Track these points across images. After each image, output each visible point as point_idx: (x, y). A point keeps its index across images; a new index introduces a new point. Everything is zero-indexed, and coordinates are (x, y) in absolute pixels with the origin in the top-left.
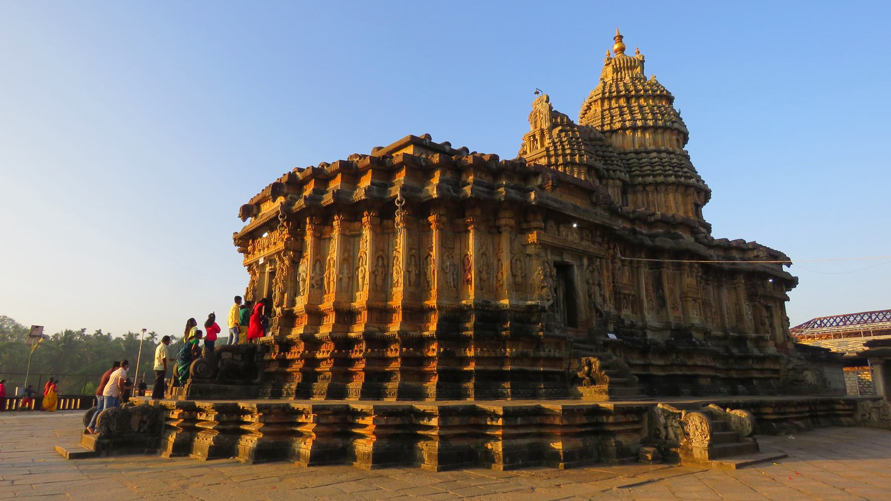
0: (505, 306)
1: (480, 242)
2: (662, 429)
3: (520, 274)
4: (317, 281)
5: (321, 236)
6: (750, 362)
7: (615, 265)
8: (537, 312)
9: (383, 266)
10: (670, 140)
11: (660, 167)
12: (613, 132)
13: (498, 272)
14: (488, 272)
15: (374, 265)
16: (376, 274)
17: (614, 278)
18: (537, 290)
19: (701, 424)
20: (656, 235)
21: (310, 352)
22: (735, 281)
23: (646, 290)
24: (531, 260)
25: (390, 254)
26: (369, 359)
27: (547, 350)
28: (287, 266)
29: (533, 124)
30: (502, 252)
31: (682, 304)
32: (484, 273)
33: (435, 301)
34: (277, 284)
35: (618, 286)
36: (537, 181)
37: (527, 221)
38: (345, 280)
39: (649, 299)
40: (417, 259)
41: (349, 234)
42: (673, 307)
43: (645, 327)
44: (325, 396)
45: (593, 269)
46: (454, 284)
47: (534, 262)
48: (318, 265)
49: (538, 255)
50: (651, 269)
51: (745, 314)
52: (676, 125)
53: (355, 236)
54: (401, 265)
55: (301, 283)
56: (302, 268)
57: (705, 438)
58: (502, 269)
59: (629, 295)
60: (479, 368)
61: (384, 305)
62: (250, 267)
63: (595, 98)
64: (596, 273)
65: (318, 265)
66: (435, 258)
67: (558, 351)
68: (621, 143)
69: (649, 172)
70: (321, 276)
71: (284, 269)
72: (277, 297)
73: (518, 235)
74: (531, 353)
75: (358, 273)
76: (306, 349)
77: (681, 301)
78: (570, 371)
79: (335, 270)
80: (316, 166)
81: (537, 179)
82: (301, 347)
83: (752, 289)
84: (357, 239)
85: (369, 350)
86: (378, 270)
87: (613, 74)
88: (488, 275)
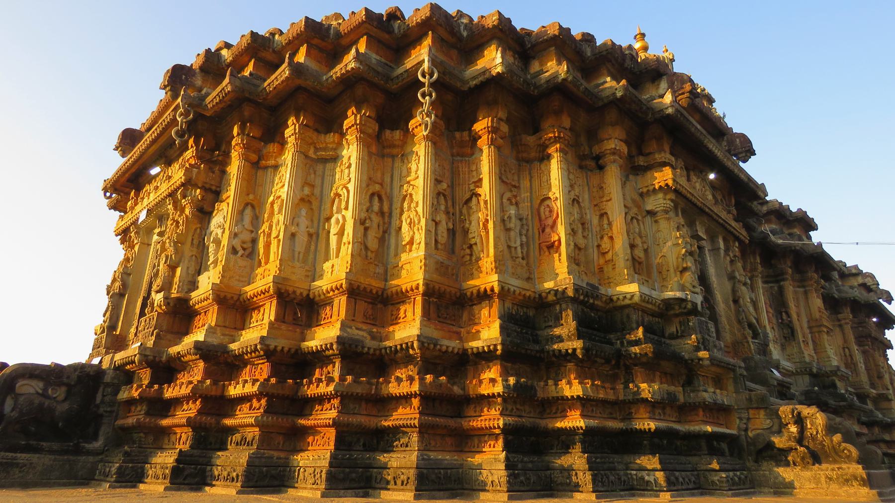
3: (640, 245)
4: (244, 242)
5: (257, 163)
8: (677, 315)
13: (602, 238)
15: (365, 208)
18: (673, 275)
21: (215, 383)
22: (840, 316)
24: (656, 222)
26: (346, 399)
28: (187, 216)
30: (610, 200)
31: (812, 337)
33: (494, 278)
37: (641, 153)
38: (301, 239)
40: (450, 203)
44: (239, 484)
46: (522, 252)
47: (663, 224)
53: (324, 161)
54: (420, 209)
56: (217, 220)
60: (593, 423)
61: (383, 287)
62: (124, 234)
66: (488, 198)
70: (253, 235)
71: (181, 222)
72: (160, 275)
73: (631, 177)
76: (207, 374)
77: (811, 333)
78: (750, 434)
79: (281, 218)
81: (659, 85)
82: (197, 372)
83: (861, 329)
84: (329, 166)
85: (349, 378)
86: (370, 218)
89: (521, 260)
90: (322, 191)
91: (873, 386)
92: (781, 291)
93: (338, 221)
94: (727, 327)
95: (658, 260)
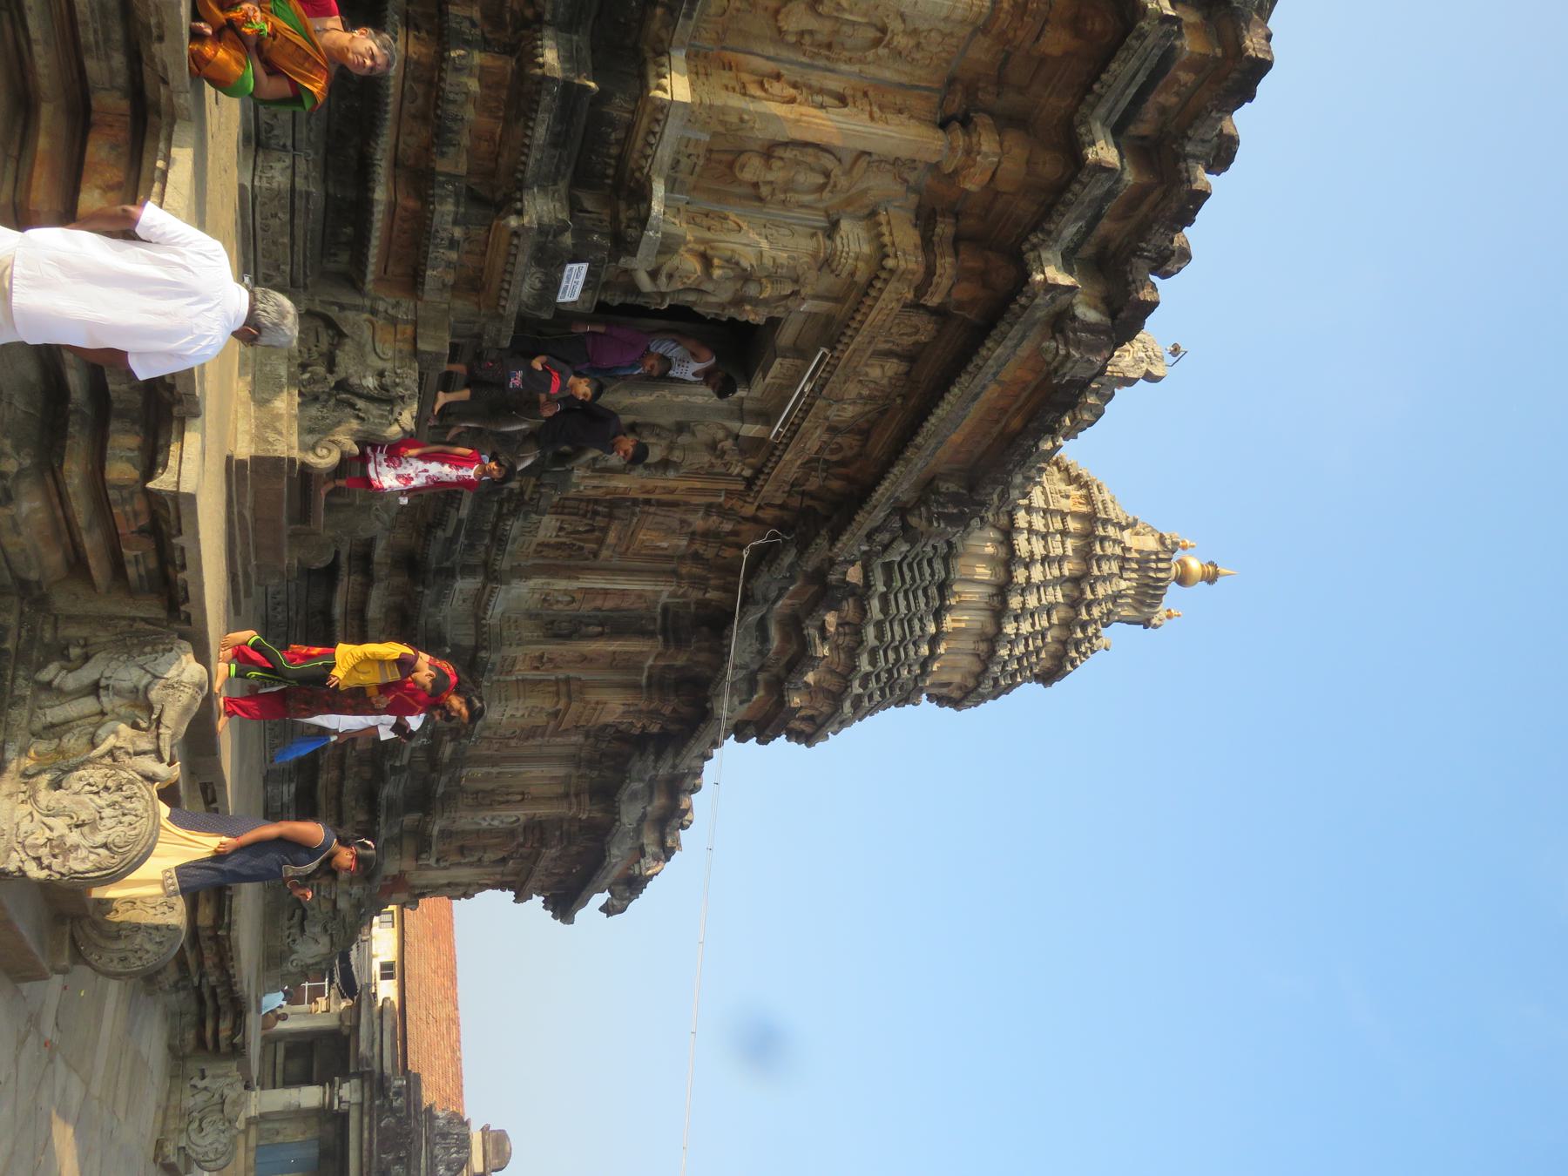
0: (665, 82)
1: (931, 30)
2: (88, 674)
3: (770, 177)
6: (362, 817)
7: (701, 514)
8: (615, 218)
10: (954, 668)
11: (898, 638)
12: (1008, 534)
13: (795, 86)
14: (807, 39)
17: (660, 504)
19: (105, 846)
20: (764, 637)
22: (585, 798)
23: (606, 593)
27: (458, 233)
30: (872, 118)
31: (549, 680)
35: (634, 514)
36: (1089, 305)
39: (579, 596)
42: (545, 659)
43: (493, 576)
45: (724, 452)
49: (826, 264)
50: (665, 609)
51: (495, 813)
52: (987, 685)
57: (38, 859)
58: (806, 102)
59: (601, 542)
64: (706, 458)
67: (450, 279)
68: (973, 550)
69: (893, 610)
73: (913, 199)
74: (452, 163)
77: (557, 681)
81: (1095, 308)
83: (558, 833)
87: (1137, 551)
88: (792, 39)
92: (643, 633)
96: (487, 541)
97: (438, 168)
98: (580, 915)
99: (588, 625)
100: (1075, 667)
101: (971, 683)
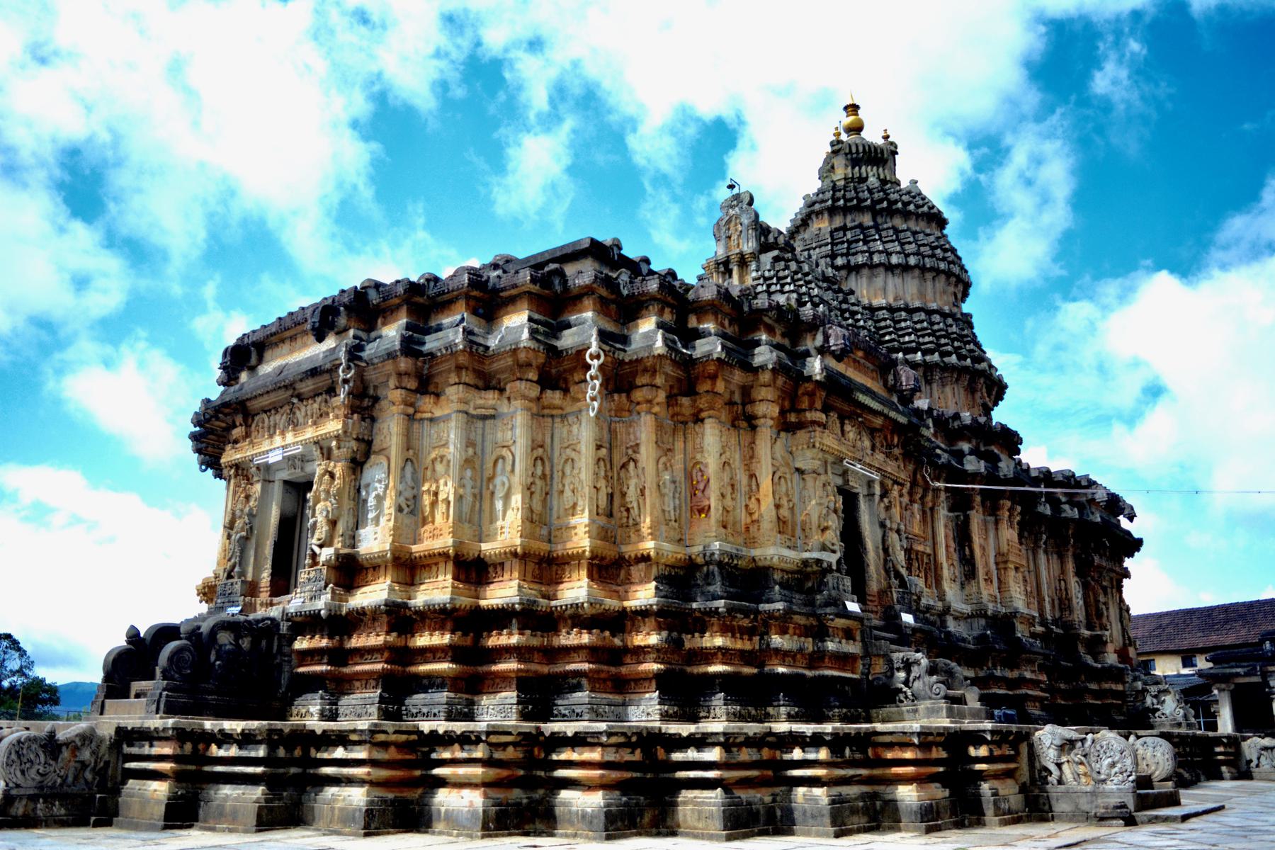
0: (769, 558)
2: (1052, 768)
3: (786, 504)
4: (407, 499)
9: (544, 477)
11: (931, 339)
13: (750, 498)
16: (533, 490)
23: (947, 546)
25: (556, 453)
29: (723, 242)
32: (729, 497)
34: (317, 501)
36: (814, 339)
38: (469, 499)
39: (950, 562)
41: (474, 412)
43: (947, 610)
48: (409, 468)
55: (371, 502)
63: (817, 207)
65: (409, 468)
73: (783, 434)
75: (495, 486)
77: (997, 569)
78: (870, 678)
80: (414, 278)
89: (673, 523)
90: (483, 450)
91: (1090, 626)
92: (967, 519)
93: (503, 484)
94: (875, 576)
95: (803, 518)
96: (928, 615)
97: (811, 649)
98: (1136, 535)
99: (965, 555)
100: (933, 207)
101: (953, 280)
